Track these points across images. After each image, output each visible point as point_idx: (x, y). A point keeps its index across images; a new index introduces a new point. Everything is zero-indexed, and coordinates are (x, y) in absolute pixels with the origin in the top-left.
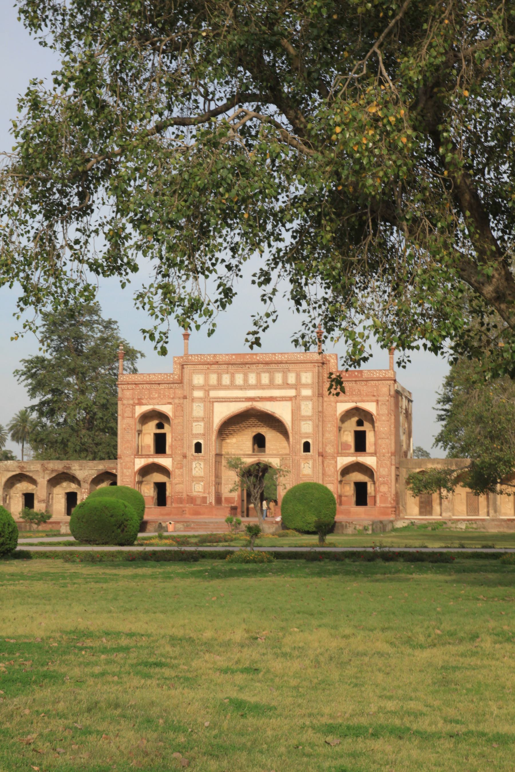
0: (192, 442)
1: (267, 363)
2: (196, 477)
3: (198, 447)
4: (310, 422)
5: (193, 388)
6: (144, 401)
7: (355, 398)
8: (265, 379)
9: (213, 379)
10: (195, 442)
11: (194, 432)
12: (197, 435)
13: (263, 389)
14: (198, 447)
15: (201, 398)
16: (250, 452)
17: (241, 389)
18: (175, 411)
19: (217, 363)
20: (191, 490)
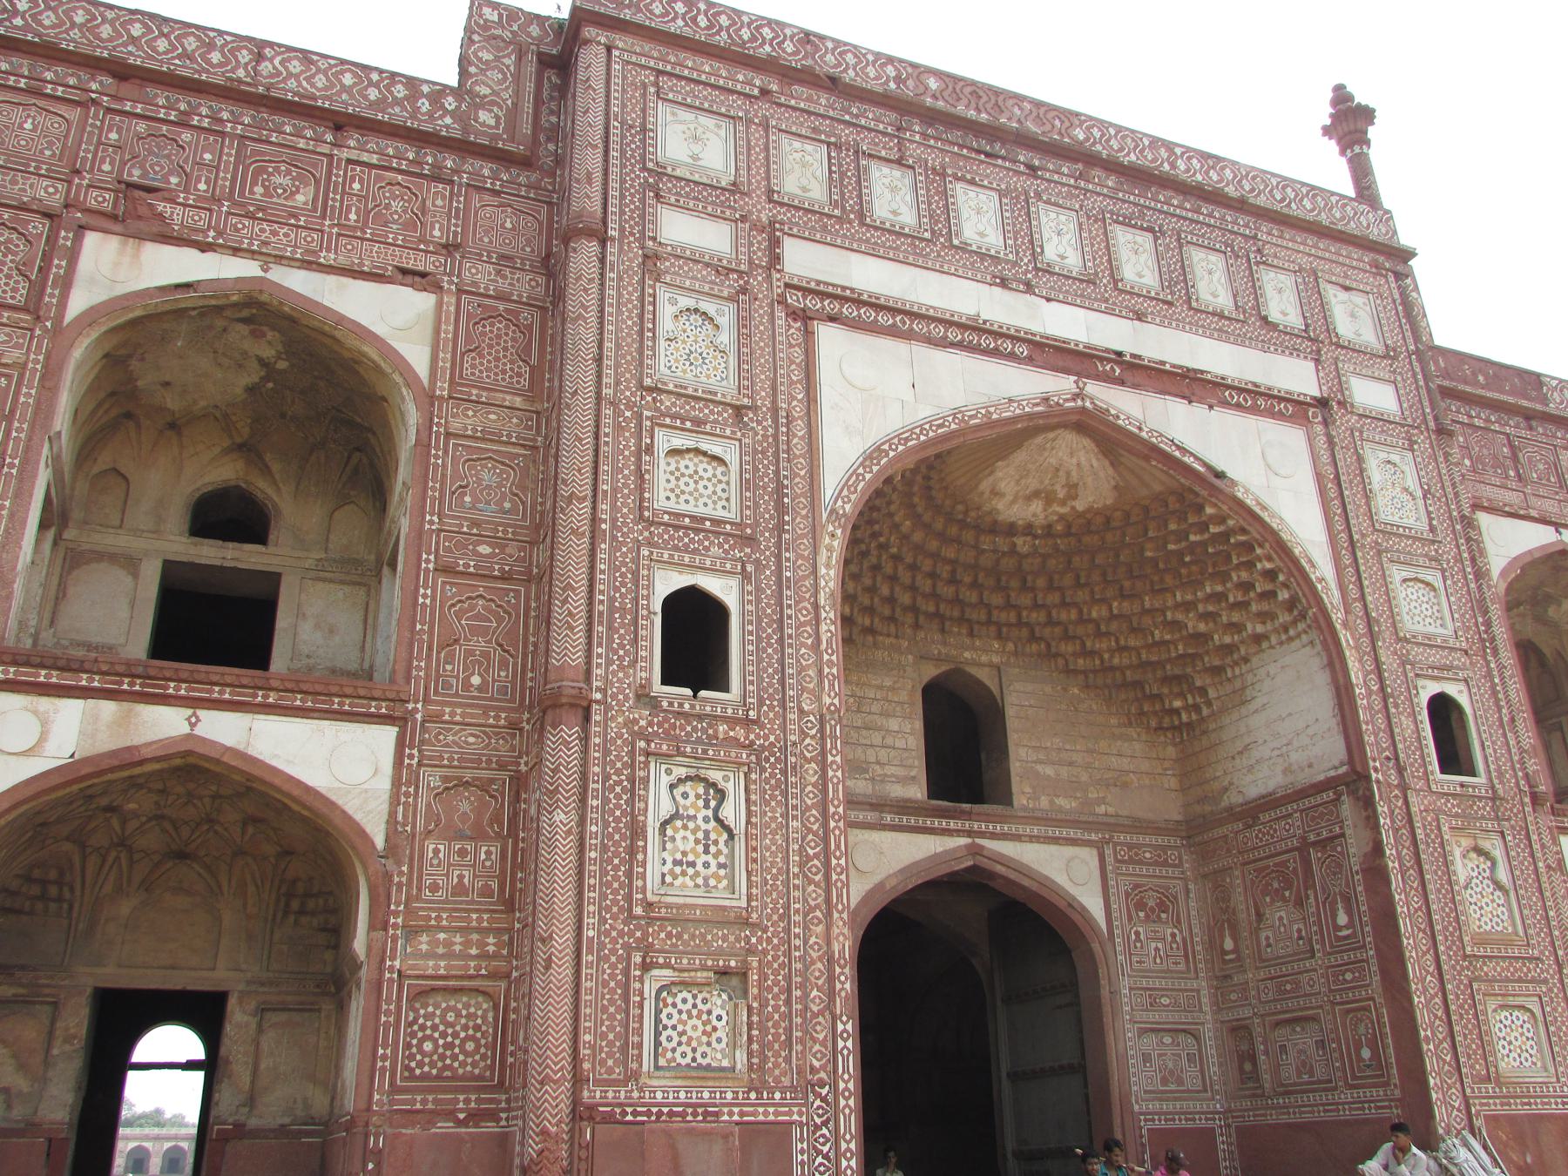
0: (638, 582)
1: (1140, 177)
2: (680, 918)
3: (694, 639)
4: (1434, 577)
5: (661, 184)
6: (177, 216)
7: (1550, 507)
8: (1137, 261)
9: (803, 170)
10: (667, 582)
11: (662, 498)
12: (693, 530)
13: (1140, 317)
14: (694, 639)
15: (721, 269)
16: (917, 791)
17: (1004, 283)
18: (457, 344)
19: (833, 84)
20: (627, 1047)
